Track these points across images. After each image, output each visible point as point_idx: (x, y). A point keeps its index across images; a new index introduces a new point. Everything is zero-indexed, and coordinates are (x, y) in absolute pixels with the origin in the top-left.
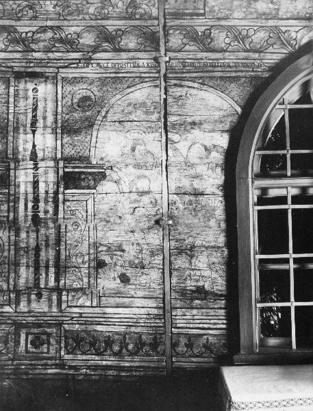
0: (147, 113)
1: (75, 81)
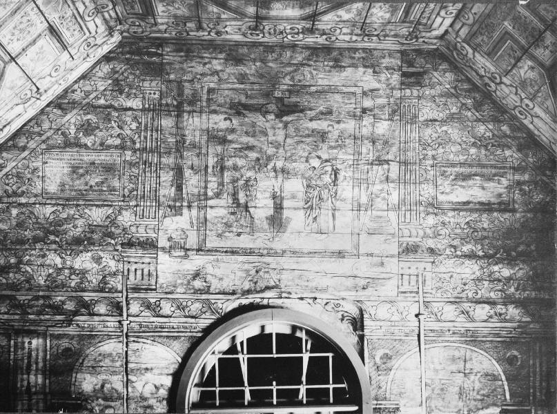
0: (113, 361)
1: (59, 337)
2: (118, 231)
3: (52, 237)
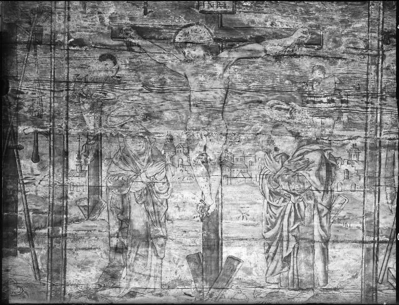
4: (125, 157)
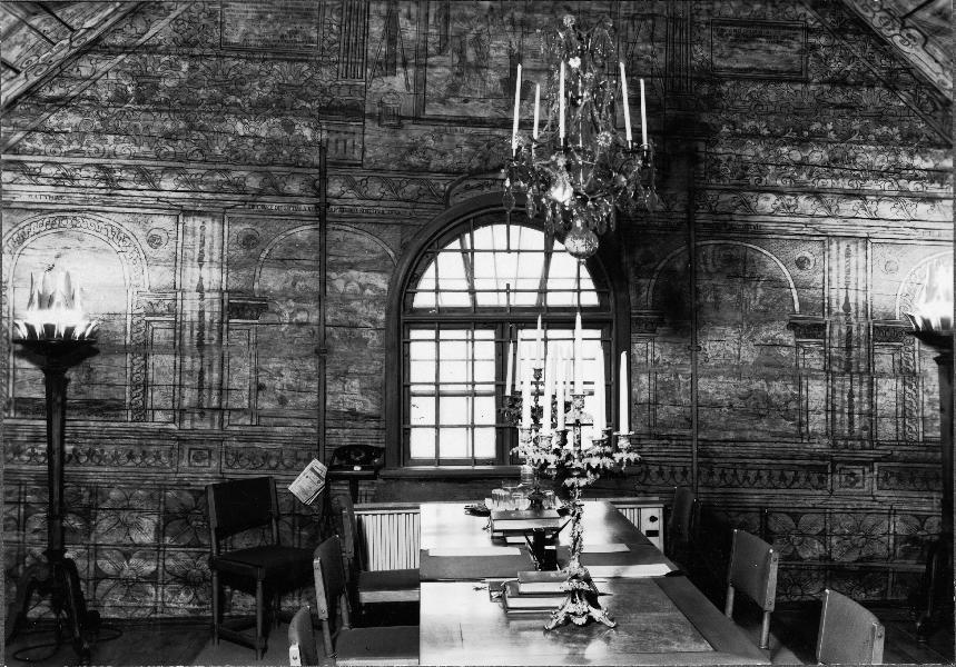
2: (317, 93)
3: (232, 98)
4: (464, 18)
